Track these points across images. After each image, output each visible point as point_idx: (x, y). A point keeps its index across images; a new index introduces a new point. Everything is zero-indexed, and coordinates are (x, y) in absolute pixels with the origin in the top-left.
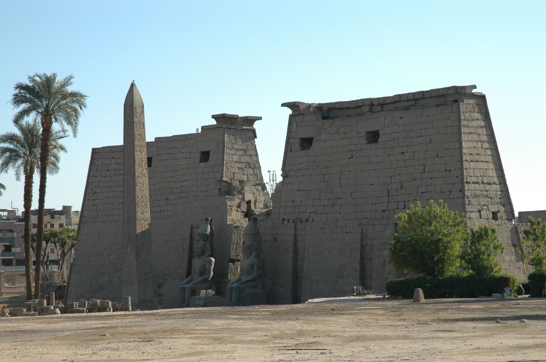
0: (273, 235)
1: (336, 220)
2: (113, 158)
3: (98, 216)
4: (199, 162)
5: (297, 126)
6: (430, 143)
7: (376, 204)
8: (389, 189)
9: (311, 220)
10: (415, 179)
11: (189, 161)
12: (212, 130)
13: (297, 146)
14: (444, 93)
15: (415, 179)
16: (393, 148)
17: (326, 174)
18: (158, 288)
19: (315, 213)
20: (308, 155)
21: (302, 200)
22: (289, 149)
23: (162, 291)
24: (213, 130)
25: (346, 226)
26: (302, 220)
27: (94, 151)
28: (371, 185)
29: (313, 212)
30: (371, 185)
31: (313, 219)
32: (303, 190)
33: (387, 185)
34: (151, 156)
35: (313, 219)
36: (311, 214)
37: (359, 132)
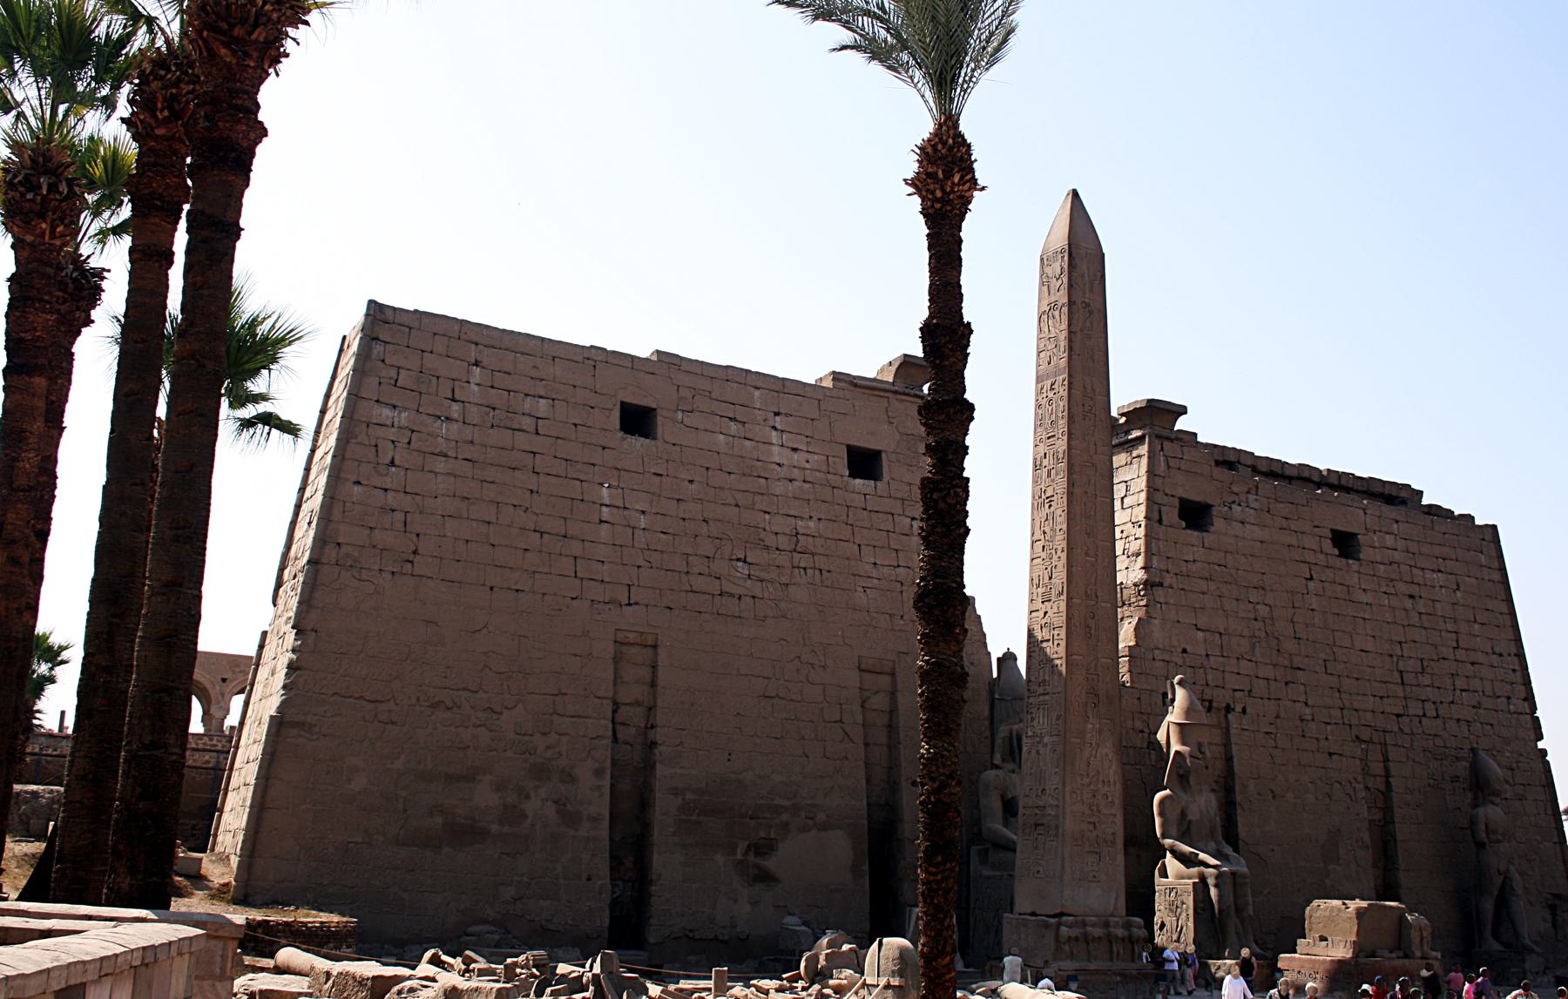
0: (1142, 731)
1: (1302, 720)
2: (477, 364)
3: (415, 552)
4: (847, 473)
5: (1169, 467)
6: (1458, 589)
7: (1381, 697)
8: (1401, 668)
9: (1239, 708)
10: (1444, 658)
11: (808, 462)
12: (876, 393)
13: (1171, 514)
14: (1394, 493)
15: (1444, 658)
16: (1392, 580)
17: (1258, 603)
18: (751, 854)
19: (1246, 693)
20: (1206, 545)
21: (1207, 655)
22: (1156, 516)
23: (771, 863)
24: (882, 394)
25: (1327, 739)
26: (1214, 704)
27: (378, 314)
28: (1362, 651)
29: (1243, 691)
30: (1362, 651)
31: (1244, 711)
32: (1208, 631)
33: (1395, 659)
34: (654, 406)
35: (1244, 711)
36: (1237, 694)
37: (1316, 523)
